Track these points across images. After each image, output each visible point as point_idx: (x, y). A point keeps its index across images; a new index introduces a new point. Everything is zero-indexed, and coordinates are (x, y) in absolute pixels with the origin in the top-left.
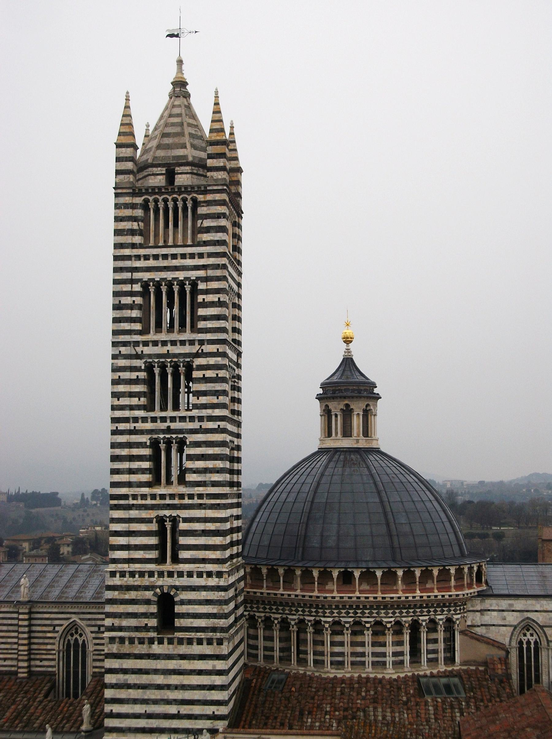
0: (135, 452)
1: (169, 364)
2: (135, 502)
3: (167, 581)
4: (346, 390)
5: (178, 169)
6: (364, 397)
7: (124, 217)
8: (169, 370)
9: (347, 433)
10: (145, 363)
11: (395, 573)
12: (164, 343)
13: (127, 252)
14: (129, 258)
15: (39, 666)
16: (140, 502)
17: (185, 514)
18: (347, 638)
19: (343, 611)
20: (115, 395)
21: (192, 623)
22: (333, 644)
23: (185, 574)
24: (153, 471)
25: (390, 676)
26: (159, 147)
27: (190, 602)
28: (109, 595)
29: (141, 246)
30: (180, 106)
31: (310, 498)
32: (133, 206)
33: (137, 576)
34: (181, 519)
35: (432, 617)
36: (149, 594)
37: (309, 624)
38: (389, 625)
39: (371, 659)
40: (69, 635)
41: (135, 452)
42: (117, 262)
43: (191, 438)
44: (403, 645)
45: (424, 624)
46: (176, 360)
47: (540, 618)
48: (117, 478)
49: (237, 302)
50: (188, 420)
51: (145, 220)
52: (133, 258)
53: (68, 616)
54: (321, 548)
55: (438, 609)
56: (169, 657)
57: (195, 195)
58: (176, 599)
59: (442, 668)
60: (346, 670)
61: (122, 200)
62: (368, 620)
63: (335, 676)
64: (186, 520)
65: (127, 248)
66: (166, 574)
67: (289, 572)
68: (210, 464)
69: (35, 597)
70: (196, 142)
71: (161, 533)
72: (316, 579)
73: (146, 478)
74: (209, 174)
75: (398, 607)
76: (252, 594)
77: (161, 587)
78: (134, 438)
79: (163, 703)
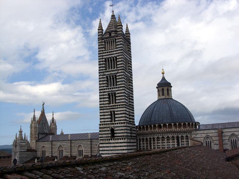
0: (105, 97)
3: (112, 126)
8: (111, 77)
9: (163, 95)
10: (106, 76)
12: (110, 71)
14: (102, 53)
17: (116, 110)
18: (160, 141)
27: (118, 130)
29: (104, 51)
32: (102, 42)
36: (108, 129)
41: (105, 97)
51: (105, 45)
54: (154, 120)
56: (113, 143)
61: (100, 41)
64: (116, 111)
67: (147, 127)
68: (121, 98)
71: (111, 115)
73: (107, 102)
74: (118, 33)
75: (173, 133)
77: (111, 127)
78: (104, 94)
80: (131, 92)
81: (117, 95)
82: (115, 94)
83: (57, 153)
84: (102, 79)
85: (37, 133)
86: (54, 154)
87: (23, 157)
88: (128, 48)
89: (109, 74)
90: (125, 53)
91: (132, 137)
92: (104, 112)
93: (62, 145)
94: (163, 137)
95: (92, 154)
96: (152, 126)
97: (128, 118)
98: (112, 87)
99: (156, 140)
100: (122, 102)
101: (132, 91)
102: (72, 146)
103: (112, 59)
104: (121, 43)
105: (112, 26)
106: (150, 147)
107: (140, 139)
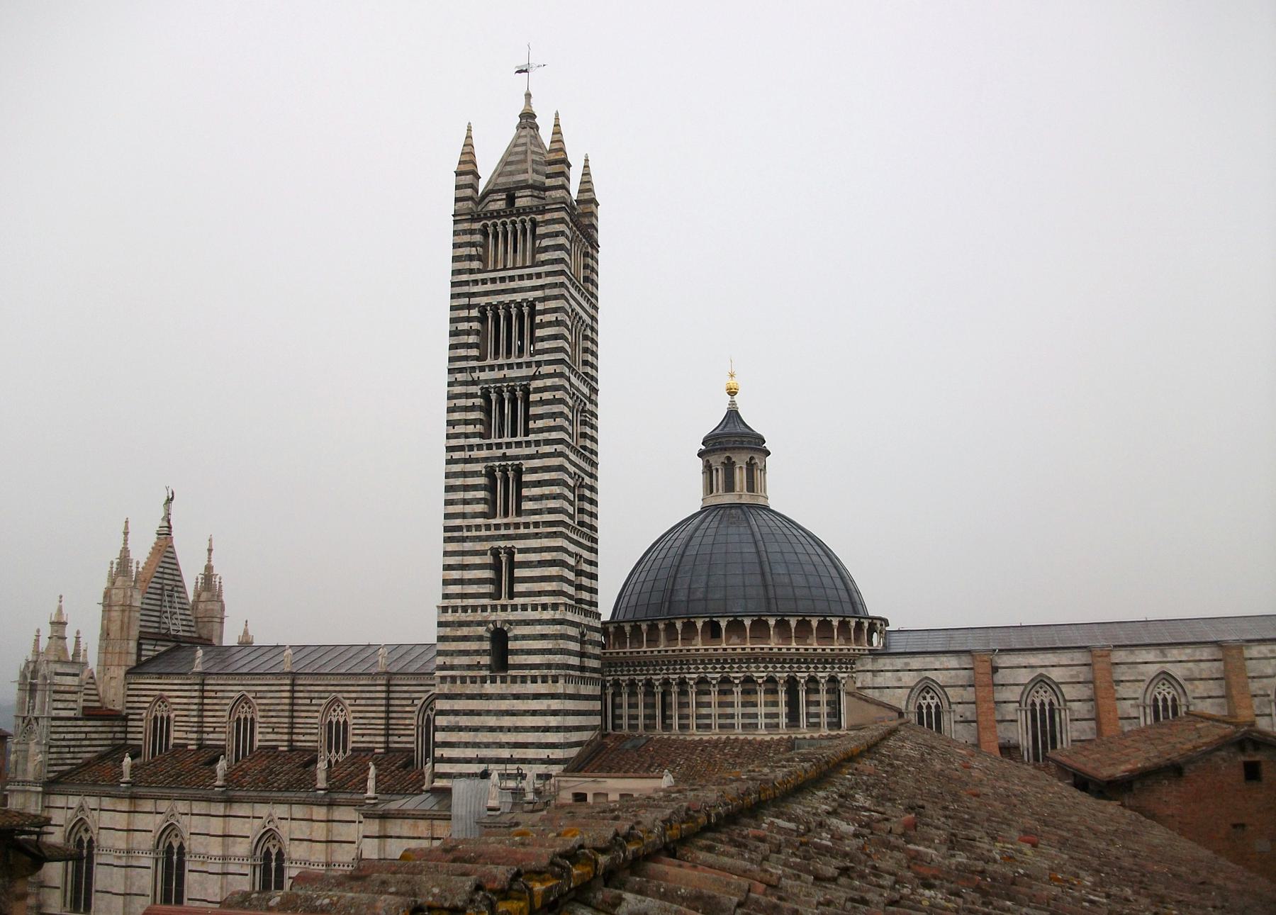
0: (470, 481)
1: (505, 389)
2: (469, 534)
3: (501, 616)
4: (728, 442)
5: (518, 194)
6: (747, 448)
7: (462, 244)
8: (506, 395)
9: (730, 487)
10: (482, 389)
11: (766, 623)
12: (501, 367)
13: (464, 277)
14: (467, 283)
15: (397, 742)
16: (474, 533)
17: (520, 544)
18: (714, 698)
19: (710, 666)
20: (450, 423)
21: (525, 660)
22: (699, 705)
23: (519, 607)
24: (490, 502)
25: (762, 737)
27: (524, 637)
29: (479, 271)
30: (526, 136)
31: (680, 552)
32: (472, 232)
33: (469, 611)
34: (516, 550)
35: (813, 674)
36: (481, 630)
37: (674, 683)
38: (760, 681)
39: (741, 721)
40: (428, 710)
41: (470, 481)
42: (454, 289)
43: (527, 464)
44: (778, 706)
45: (802, 681)
46: (512, 384)
47: (940, 677)
49: (590, 335)
50: (524, 445)
51: (484, 246)
52: (471, 284)
53: (427, 688)
54: (688, 602)
55: (819, 666)
56: (502, 697)
57: (533, 216)
58: (509, 635)
59: (825, 731)
60: (713, 731)
63: (701, 739)
64: (521, 551)
65: (465, 274)
66: (499, 608)
67: (653, 628)
68: (546, 490)
71: (496, 567)
72: (680, 632)
73: (480, 508)
74: (547, 193)
75: (771, 661)
76: (614, 655)
77: (494, 622)
79: (494, 746)
80: (588, 468)
81: (526, 478)
82: (519, 471)
83: (227, 730)
84: (462, 402)
85: (135, 632)
86: (211, 736)
87: (64, 743)
88: (586, 266)
90: (572, 290)
91: (587, 674)
92: (463, 553)
93: (250, 696)
94: (725, 680)
95: (391, 745)
96: (679, 625)
97: (570, 582)
98: (506, 440)
99: (692, 691)
100: (551, 511)
101: (594, 465)
102: (300, 701)
103: (514, 311)
104: (561, 240)
106: (663, 722)
107: (617, 684)
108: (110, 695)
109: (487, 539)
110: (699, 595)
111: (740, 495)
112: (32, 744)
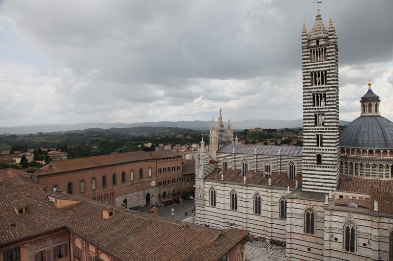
0: (310, 117)
3: (319, 151)
5: (320, 40)
8: (319, 95)
9: (370, 111)
14: (307, 66)
16: (311, 131)
18: (371, 168)
22: (366, 170)
26: (314, 35)
27: (326, 157)
28: (303, 154)
29: (310, 62)
32: (307, 52)
36: (314, 155)
41: (310, 117)
43: (326, 114)
48: (305, 124)
51: (311, 55)
56: (320, 171)
61: (304, 50)
62: (378, 164)
64: (324, 135)
68: (331, 120)
69: (282, 154)
70: (325, 32)
71: (318, 139)
78: (309, 114)
85: (217, 143)
89: (316, 92)
103: (320, 73)
105: (318, 31)
108: (213, 157)
109: (315, 132)
110: (366, 142)
111: (373, 113)
112: (200, 171)
